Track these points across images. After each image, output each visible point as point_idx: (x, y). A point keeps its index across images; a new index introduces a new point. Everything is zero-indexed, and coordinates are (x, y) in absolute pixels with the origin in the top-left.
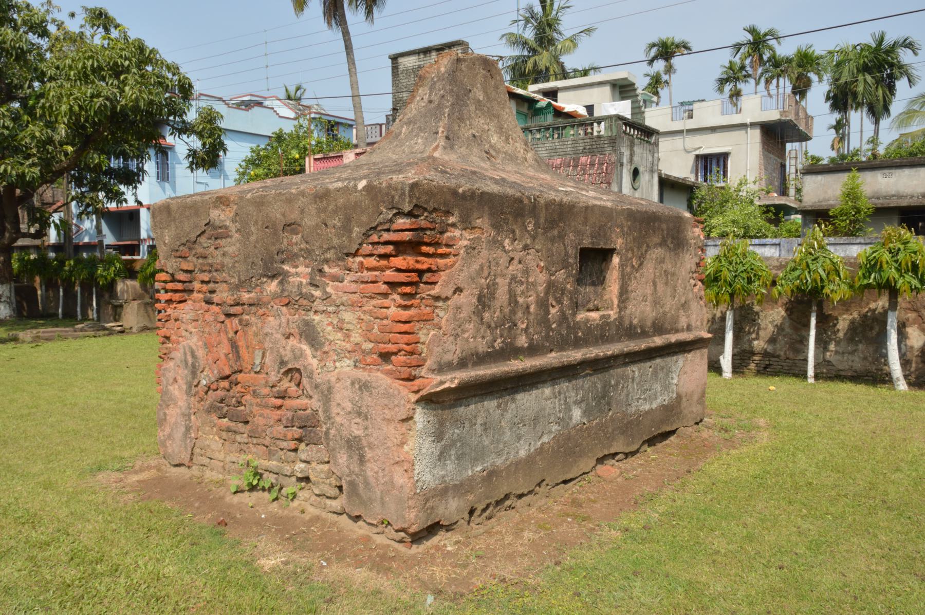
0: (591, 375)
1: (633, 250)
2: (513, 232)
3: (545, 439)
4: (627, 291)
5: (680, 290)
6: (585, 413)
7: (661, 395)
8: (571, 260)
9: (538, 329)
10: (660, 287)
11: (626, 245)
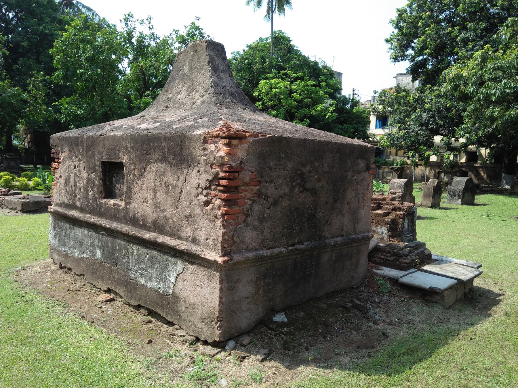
0: (106, 236)
1: (135, 164)
2: (75, 153)
3: (85, 255)
4: (131, 192)
5: (184, 202)
6: (102, 255)
7: (156, 282)
8: (97, 168)
9: (84, 200)
10: (161, 196)
11: (130, 160)
